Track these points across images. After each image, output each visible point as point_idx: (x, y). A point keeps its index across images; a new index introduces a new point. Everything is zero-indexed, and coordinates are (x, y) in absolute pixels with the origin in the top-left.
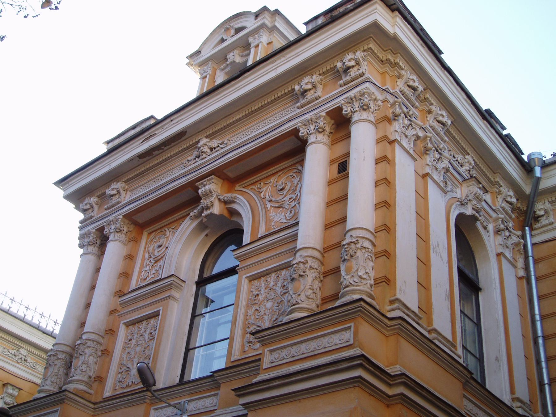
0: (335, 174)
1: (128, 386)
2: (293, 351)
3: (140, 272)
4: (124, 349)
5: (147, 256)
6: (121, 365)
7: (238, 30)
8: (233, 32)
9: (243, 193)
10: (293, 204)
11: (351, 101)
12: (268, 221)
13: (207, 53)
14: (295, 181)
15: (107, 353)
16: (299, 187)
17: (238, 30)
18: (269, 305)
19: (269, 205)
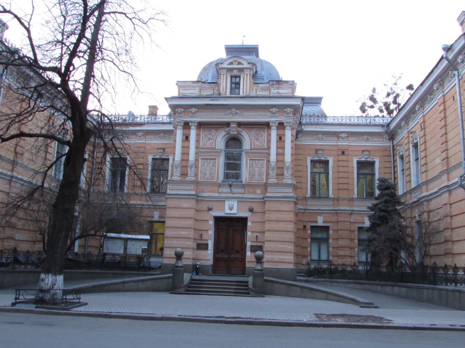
0: (278, 140)
1: (207, 179)
2: (276, 189)
3: (202, 141)
4: (201, 166)
5: (204, 136)
6: (201, 171)
7: (239, 63)
8: (237, 63)
9: (243, 129)
10: (262, 141)
11: (287, 123)
12: (254, 143)
13: (225, 65)
14: (263, 134)
15: (197, 167)
16: (264, 136)
17: (239, 63)
18: (257, 169)
19: (253, 137)
